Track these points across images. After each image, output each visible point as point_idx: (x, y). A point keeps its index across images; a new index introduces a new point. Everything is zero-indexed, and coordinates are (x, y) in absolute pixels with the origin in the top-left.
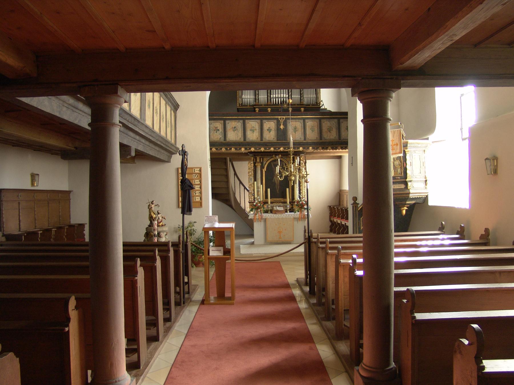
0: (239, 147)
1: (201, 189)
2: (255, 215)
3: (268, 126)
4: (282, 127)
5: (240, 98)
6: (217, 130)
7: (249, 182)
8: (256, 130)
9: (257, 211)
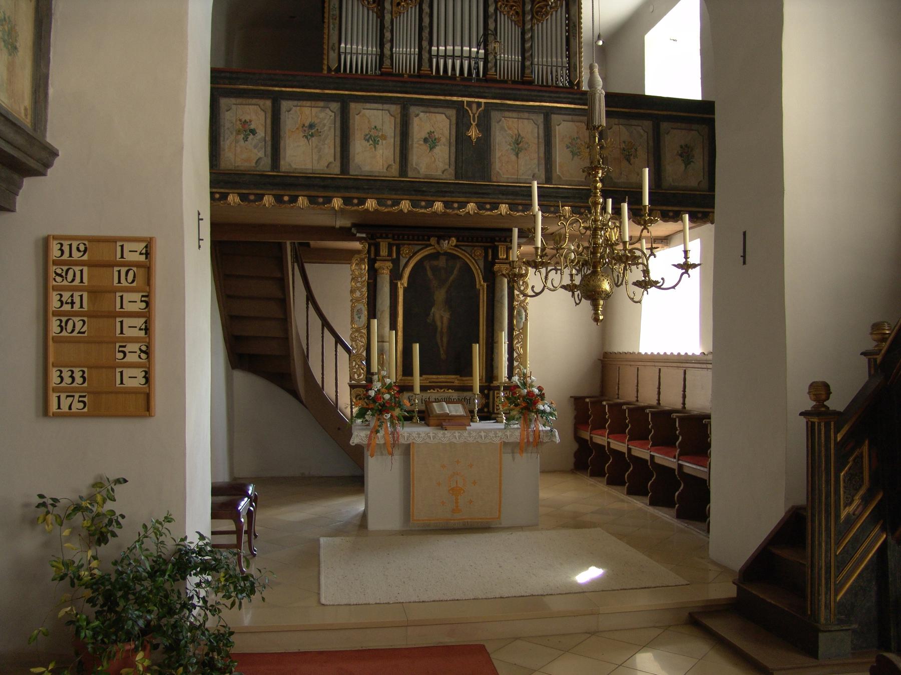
0: (326, 194)
1: (149, 337)
2: (372, 432)
3: (427, 128)
5: (331, 53)
6: (248, 131)
7: (352, 322)
8: (384, 137)
9: (379, 419)
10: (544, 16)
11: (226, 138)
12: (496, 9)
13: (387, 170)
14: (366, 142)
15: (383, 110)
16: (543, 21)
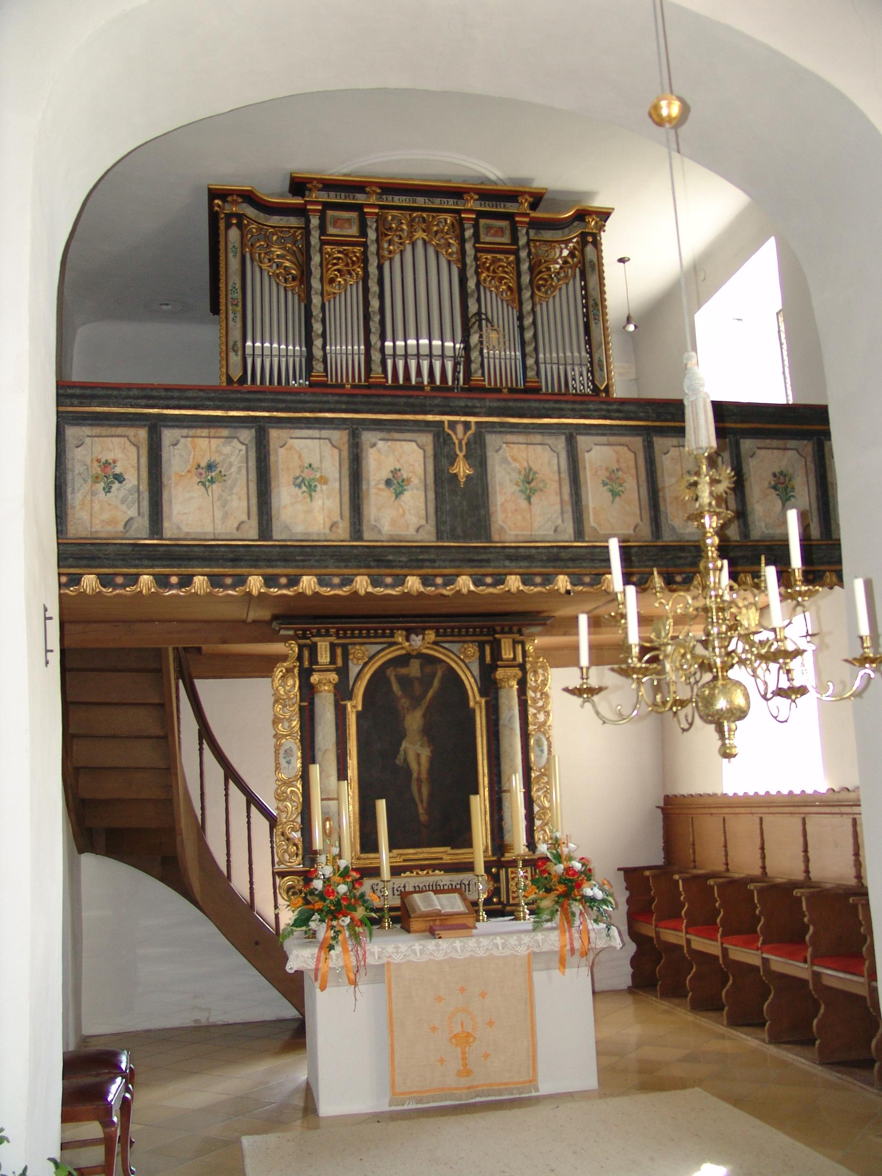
0: (238, 571)
2: (321, 948)
4: (462, 469)
7: (278, 768)
8: (324, 480)
10: (549, 292)
11: (76, 488)
12: (478, 284)
13: (331, 530)
14: (297, 488)
15: (320, 439)
16: (548, 298)
